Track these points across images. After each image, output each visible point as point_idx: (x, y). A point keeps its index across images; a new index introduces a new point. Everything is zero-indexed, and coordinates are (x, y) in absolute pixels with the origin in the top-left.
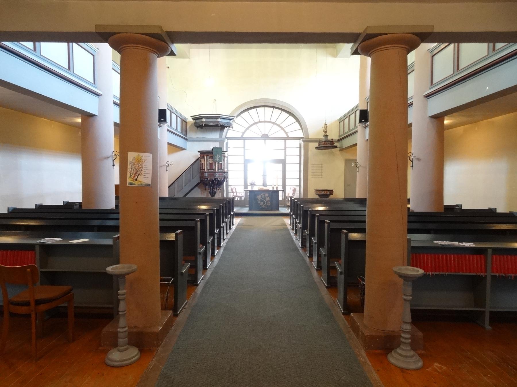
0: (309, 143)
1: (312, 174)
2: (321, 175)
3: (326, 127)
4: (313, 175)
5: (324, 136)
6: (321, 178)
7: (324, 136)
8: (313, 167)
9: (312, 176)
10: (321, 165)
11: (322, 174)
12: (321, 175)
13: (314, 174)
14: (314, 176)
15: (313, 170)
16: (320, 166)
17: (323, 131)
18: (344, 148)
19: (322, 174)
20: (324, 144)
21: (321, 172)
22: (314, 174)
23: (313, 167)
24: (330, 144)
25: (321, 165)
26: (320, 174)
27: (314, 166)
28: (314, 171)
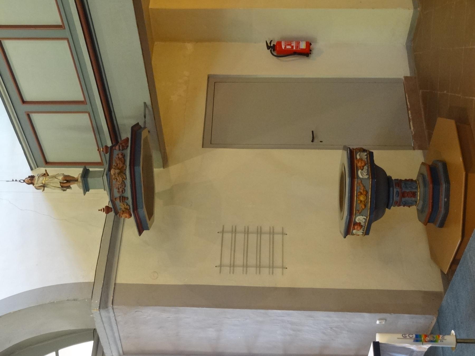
0: (119, 281)
1: (265, 271)
2: (272, 233)
3: (43, 180)
4: (272, 267)
5: (86, 189)
6: (283, 234)
7: (86, 189)
8: (233, 266)
9: (278, 271)
10: (223, 232)
11: (266, 229)
12: (272, 233)
13: (265, 260)
14: (278, 262)
15: (246, 266)
16: (228, 236)
17: (59, 191)
18: (149, 103)
19: (266, 229)
20: (122, 172)
21: (259, 232)
22: (265, 260)
23: (233, 266)
24: (124, 148)
25: (223, 232)
26: (266, 238)
27: (226, 261)
28: (252, 261)
